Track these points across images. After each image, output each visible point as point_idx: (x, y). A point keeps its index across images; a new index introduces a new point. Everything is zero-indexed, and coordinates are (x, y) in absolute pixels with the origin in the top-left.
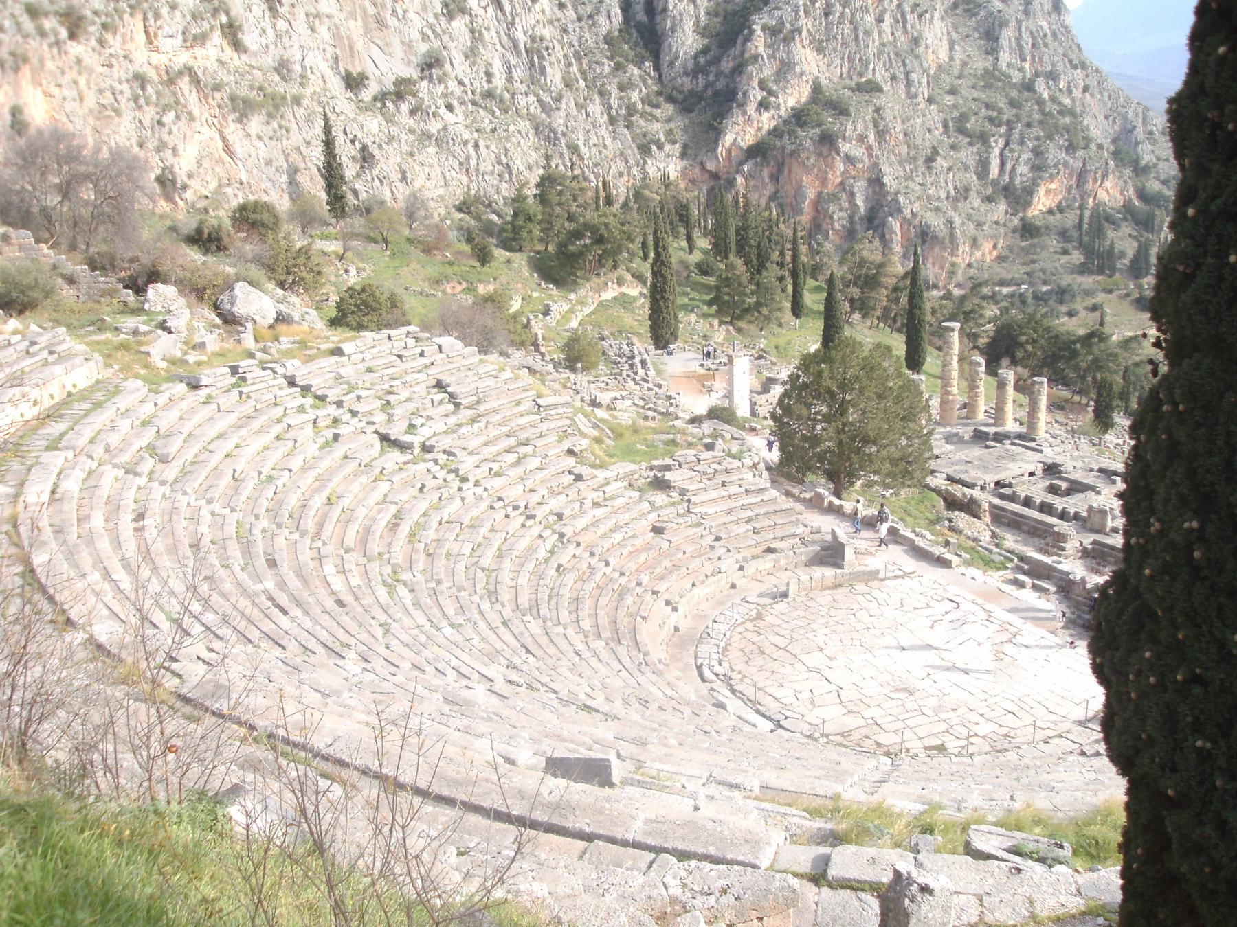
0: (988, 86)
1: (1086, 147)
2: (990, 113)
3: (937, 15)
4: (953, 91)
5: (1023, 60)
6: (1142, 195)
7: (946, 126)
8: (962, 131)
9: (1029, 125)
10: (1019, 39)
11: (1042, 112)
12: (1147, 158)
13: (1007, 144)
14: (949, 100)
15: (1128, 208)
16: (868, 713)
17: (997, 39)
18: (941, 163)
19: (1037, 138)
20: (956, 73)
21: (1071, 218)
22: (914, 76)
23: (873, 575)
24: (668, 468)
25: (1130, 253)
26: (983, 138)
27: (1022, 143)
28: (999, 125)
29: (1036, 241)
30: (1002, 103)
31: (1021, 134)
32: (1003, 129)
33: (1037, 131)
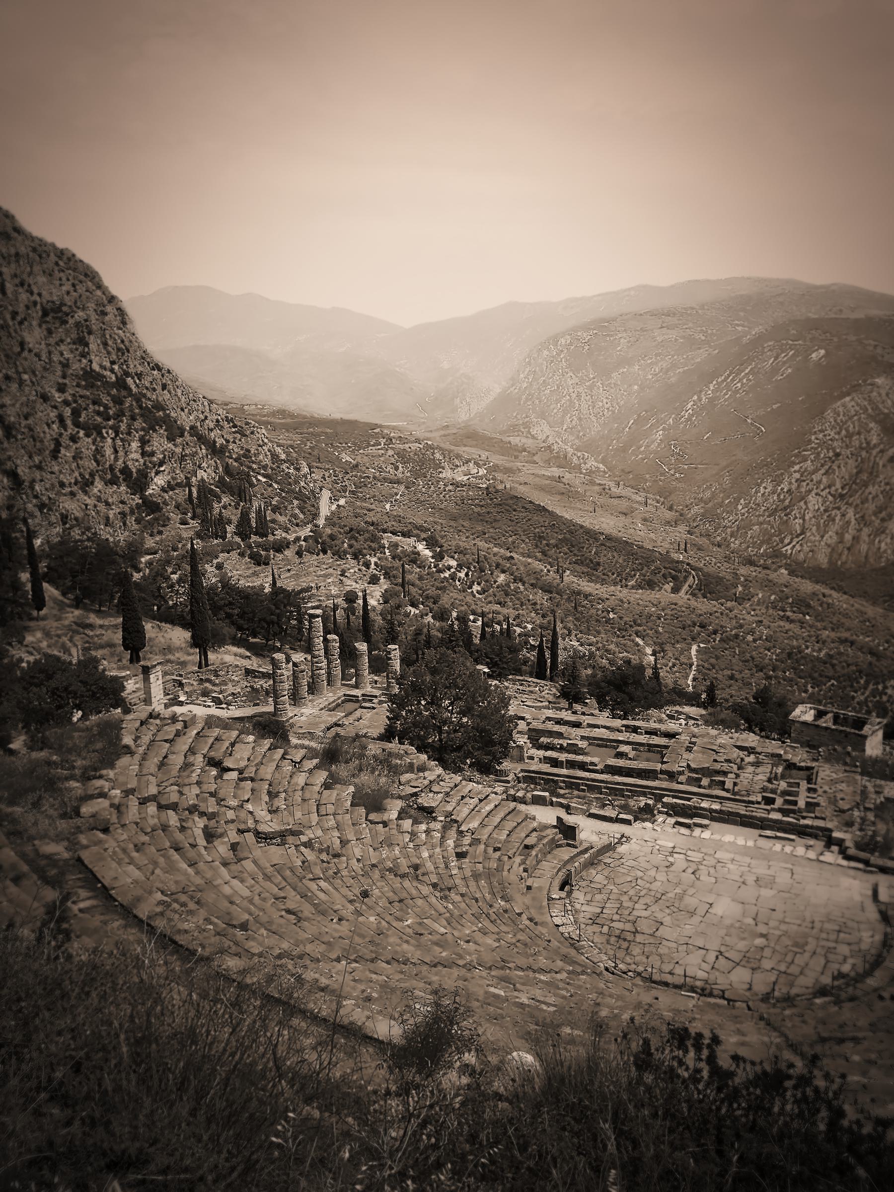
0: (92, 386)
1: (182, 435)
2: (97, 408)
3: (35, 323)
4: (62, 389)
5: (113, 363)
6: (227, 470)
7: (61, 419)
8: (77, 424)
9: (133, 418)
10: (105, 344)
11: (141, 407)
12: (220, 441)
13: (117, 435)
14: (58, 397)
15: (221, 483)
16: (767, 964)
17: (87, 345)
18: (66, 454)
19: (143, 429)
20: (59, 373)
21: (181, 495)
22: (25, 377)
23: (609, 848)
24: (415, 795)
25: (235, 519)
26: (98, 429)
27: (129, 433)
28: (109, 420)
29: (157, 515)
30: (106, 399)
31: (129, 426)
32: (111, 423)
33: (139, 423)
